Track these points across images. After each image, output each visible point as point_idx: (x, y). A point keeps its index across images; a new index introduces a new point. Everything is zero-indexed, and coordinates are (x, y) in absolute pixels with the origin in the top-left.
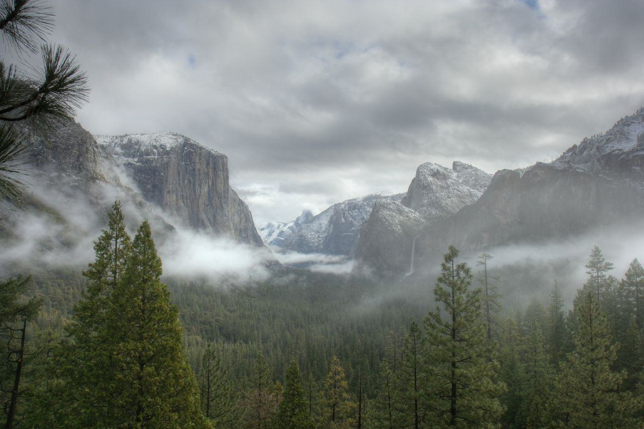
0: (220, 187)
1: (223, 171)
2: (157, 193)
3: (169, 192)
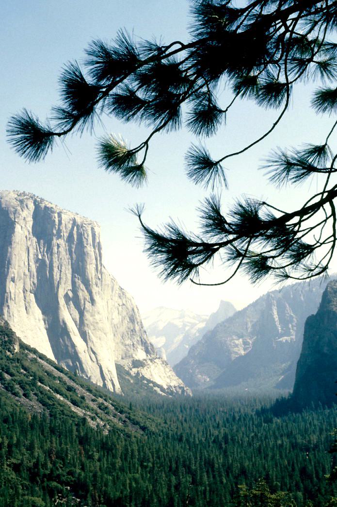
0: (91, 270)
1: (94, 247)
3: (13, 280)
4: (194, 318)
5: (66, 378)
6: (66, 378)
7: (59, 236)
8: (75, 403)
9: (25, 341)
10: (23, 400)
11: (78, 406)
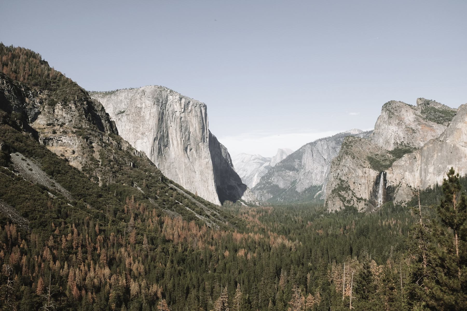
2: (145, 141)
4: (262, 160)
5: (190, 197)
6: (190, 197)
8: (197, 212)
10: (169, 211)
11: (201, 215)
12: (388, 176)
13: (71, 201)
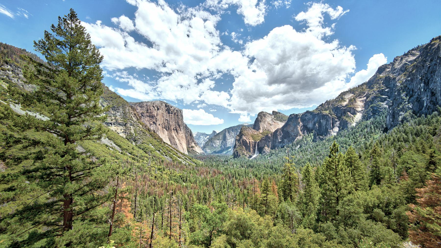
0: (180, 123)
5: (175, 151)
7: (172, 114)
8: (178, 157)
9: (165, 141)
12: (260, 143)
13: (121, 152)
